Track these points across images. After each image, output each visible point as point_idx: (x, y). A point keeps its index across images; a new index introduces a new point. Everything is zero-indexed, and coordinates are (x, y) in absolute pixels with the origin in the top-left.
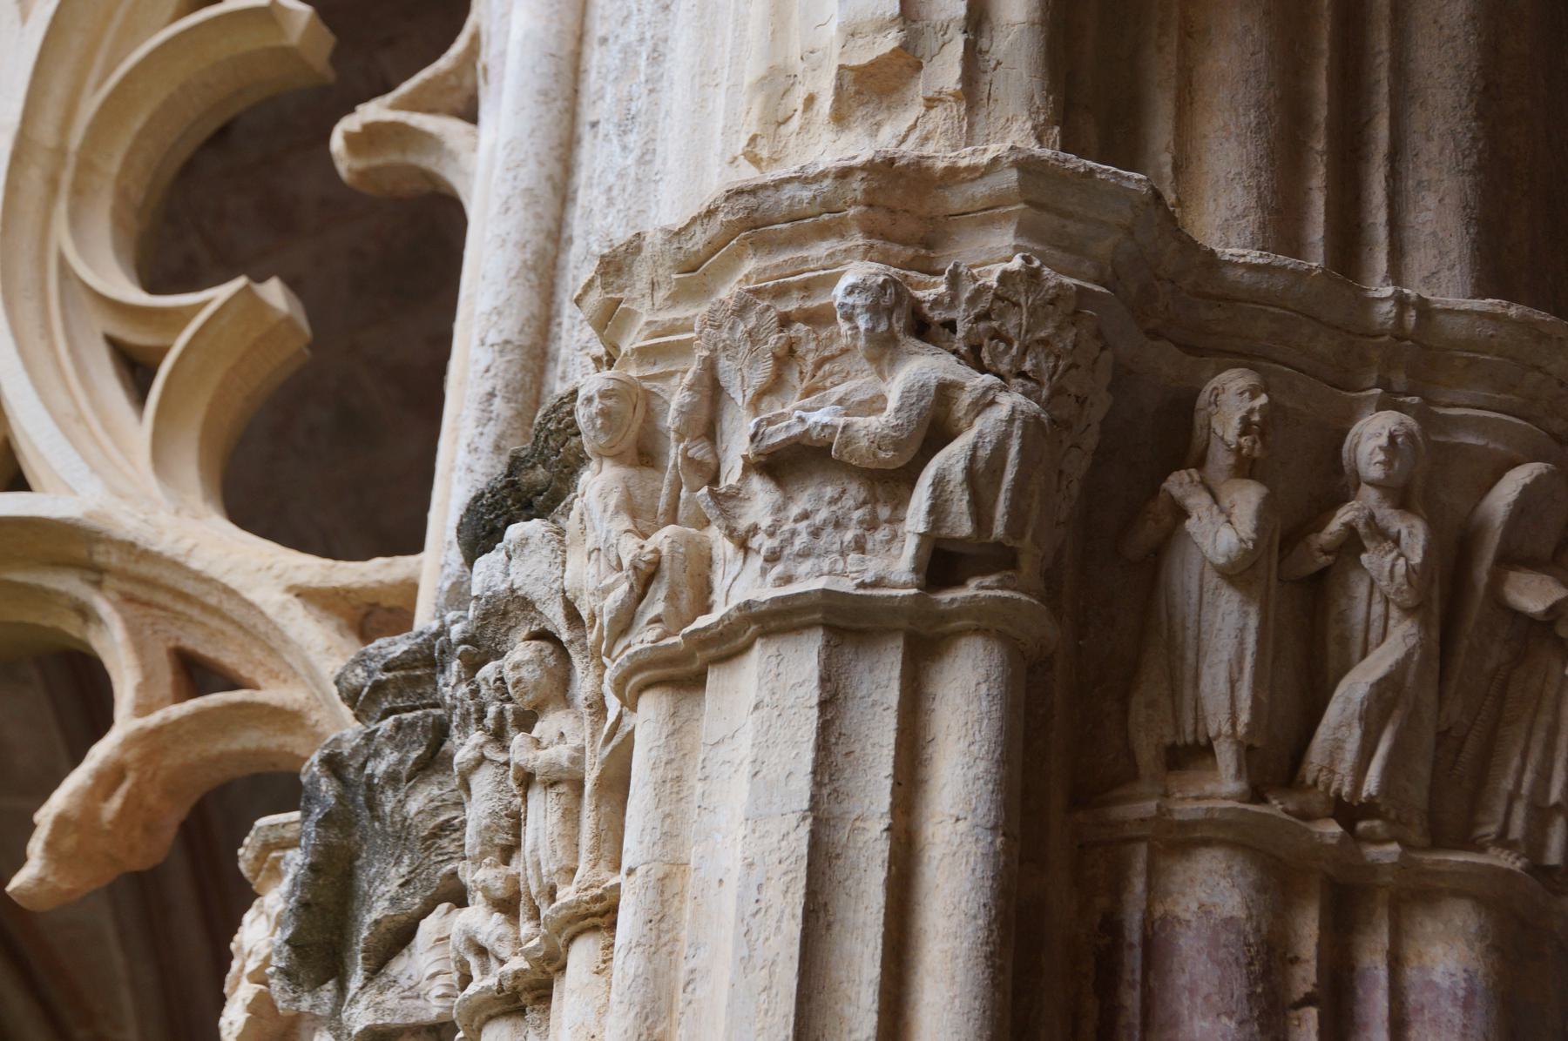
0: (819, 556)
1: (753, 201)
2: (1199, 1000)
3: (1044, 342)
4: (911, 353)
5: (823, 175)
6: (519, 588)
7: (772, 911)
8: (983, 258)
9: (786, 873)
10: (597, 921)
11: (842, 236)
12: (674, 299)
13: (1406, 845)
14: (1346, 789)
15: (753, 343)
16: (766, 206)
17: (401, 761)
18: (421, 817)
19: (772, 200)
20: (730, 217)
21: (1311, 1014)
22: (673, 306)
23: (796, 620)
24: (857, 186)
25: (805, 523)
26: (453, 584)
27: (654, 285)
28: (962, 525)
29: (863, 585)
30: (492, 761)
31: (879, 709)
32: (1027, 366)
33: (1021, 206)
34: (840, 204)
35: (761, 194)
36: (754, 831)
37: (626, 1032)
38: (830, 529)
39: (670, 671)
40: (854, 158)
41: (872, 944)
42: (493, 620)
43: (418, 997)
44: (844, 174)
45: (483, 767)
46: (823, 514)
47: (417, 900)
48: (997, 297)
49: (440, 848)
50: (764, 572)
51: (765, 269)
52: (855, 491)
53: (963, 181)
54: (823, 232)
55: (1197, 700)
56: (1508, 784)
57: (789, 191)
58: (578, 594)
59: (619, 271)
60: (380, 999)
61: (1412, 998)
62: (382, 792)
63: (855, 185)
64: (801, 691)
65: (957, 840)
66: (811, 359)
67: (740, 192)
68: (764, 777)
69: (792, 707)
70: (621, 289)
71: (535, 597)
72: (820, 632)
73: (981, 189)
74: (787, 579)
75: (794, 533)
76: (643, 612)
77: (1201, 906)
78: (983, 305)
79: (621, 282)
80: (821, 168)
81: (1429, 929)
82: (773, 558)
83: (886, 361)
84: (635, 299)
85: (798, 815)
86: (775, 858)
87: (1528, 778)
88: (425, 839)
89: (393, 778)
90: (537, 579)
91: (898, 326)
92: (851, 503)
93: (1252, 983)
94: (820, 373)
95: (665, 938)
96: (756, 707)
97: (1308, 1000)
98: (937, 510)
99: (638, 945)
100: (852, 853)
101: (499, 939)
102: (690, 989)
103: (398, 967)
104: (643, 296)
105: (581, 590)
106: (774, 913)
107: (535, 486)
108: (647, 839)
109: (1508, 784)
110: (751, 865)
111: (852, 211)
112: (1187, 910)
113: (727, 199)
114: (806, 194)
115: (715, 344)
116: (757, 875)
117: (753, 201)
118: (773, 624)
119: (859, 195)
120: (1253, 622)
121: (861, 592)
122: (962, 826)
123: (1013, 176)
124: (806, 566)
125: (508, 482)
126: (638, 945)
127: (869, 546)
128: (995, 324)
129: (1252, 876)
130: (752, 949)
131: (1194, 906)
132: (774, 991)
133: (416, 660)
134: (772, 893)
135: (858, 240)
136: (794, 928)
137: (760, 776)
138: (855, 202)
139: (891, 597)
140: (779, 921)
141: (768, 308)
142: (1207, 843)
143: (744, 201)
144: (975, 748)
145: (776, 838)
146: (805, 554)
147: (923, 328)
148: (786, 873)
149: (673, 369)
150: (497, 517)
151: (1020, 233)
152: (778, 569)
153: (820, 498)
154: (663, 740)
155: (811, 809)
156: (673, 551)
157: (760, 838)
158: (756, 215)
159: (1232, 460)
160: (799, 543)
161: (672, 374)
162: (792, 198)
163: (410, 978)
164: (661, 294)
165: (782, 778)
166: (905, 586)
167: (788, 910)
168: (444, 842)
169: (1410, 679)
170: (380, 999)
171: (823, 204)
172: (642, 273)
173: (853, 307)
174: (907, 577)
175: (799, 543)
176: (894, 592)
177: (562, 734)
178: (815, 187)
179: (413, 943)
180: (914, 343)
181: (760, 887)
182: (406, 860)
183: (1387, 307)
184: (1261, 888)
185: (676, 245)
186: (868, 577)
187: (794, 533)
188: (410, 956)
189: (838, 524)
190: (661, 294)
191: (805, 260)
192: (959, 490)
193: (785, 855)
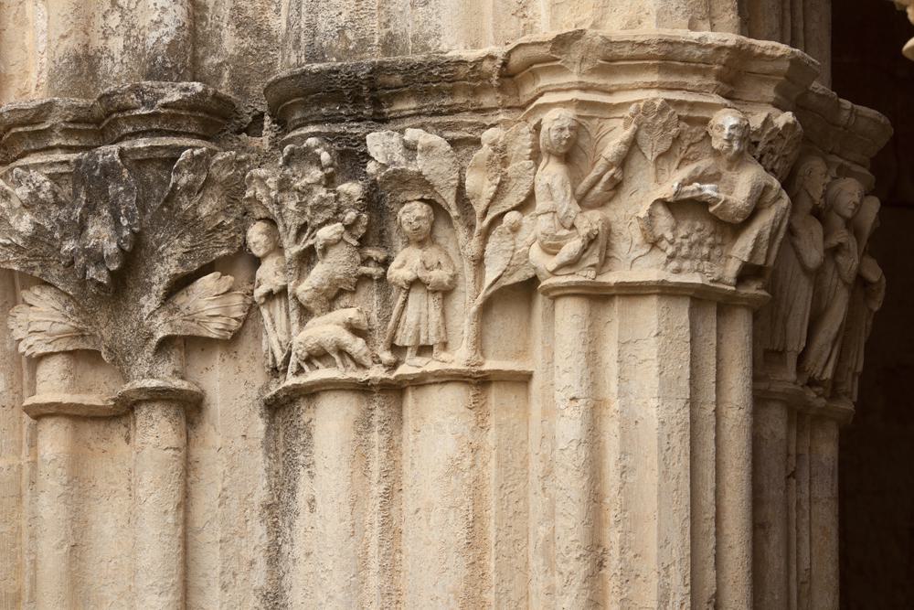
0: (692, 259)
1: (670, 48)
2: (771, 481)
3: (785, 156)
4: (747, 161)
5: (710, 46)
6: (427, 176)
7: (676, 449)
8: (759, 99)
9: (680, 431)
10: (472, 380)
11: (704, 76)
12: (593, 71)
14: (818, 374)
15: (665, 129)
16: (676, 52)
17: (195, 181)
18: (209, 218)
19: (680, 50)
20: (656, 53)
22: (590, 75)
23: (680, 292)
24: (724, 56)
25: (687, 241)
26: (172, 41)
27: (583, 60)
29: (712, 281)
30: (347, 243)
31: (707, 344)
32: (777, 167)
33: (783, 78)
34: (711, 62)
35: (675, 46)
36: (663, 404)
37: (584, 487)
38: (697, 245)
39: (594, 292)
40: (726, 41)
41: (711, 471)
42: (394, 182)
43: (193, 320)
44: (720, 49)
45: (340, 244)
46: (694, 237)
47: (196, 265)
48: (779, 134)
49: (216, 238)
50: (667, 263)
51: (664, 83)
52: (709, 227)
53: (763, 60)
54: (696, 71)
55: (785, 330)
57: (689, 48)
58: (476, 196)
59: (563, 44)
60: (170, 318)
62: (181, 195)
63: (723, 55)
64: (681, 332)
65: (740, 420)
66: (687, 143)
67: (665, 42)
68: (666, 376)
69: (677, 339)
70: (560, 54)
71: (436, 183)
72: (689, 300)
73: (769, 67)
74: (678, 271)
75: (682, 244)
76: (585, 259)
77: (772, 432)
78: (773, 137)
79: (562, 50)
80: (709, 42)
81: (821, 436)
82: (672, 257)
83: (735, 165)
84: (568, 62)
85: (685, 401)
86: (674, 421)
88: (209, 232)
89: (189, 189)
90: (438, 173)
92: (708, 233)
94: (689, 151)
95: (596, 440)
96: (657, 335)
99: (585, 442)
100: (700, 420)
101: (365, 355)
102: (624, 475)
103: (180, 300)
104: (575, 63)
105: (479, 196)
106: (677, 449)
107: (386, 84)
108: (584, 384)
110: (663, 422)
111: (716, 67)
112: (766, 434)
113: (659, 43)
114: (699, 53)
115: (642, 124)
116: (667, 429)
117: (670, 48)
118: (668, 292)
119: (723, 61)
120: (811, 295)
121: (712, 285)
122: (742, 412)
123: (787, 65)
124: (687, 264)
125: (370, 78)
126: (585, 442)
127: (712, 257)
128: (773, 146)
130: (667, 466)
131: (769, 433)
132: (680, 492)
133: (185, 106)
134: (675, 440)
135: (712, 81)
136: (686, 461)
137: (664, 374)
138: (719, 63)
139: (724, 290)
140: (679, 456)
141: (674, 112)
142: (774, 400)
143: (665, 47)
144: (746, 370)
145: (674, 411)
146: (685, 258)
148: (680, 431)
149: (596, 115)
150: (347, 88)
151: (777, 89)
152: (674, 264)
153: (693, 227)
154: (586, 330)
155: (690, 399)
156: (603, 229)
157: (667, 408)
158: (669, 55)
159: (810, 207)
160: (684, 251)
161: (593, 118)
162: (691, 52)
163: (188, 308)
164: (586, 66)
165: (675, 378)
166: (730, 285)
167: (683, 451)
168: (219, 235)
170: (170, 318)
171: (704, 59)
172: (576, 53)
173: (734, 135)
174: (732, 281)
175: (684, 251)
176: (726, 287)
177: (439, 263)
178: (703, 50)
179: (190, 287)
181: (669, 435)
182: (188, 238)
183: (846, 114)
185: (609, 48)
186: (715, 277)
187: (682, 244)
188: (188, 295)
189: (700, 243)
190: (586, 66)
191: (686, 84)
192: (765, 243)
193: (679, 421)
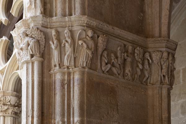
13: (72, 69)
21: (66, 84)
28: (31, 53)
56: (80, 60)
61: (75, 81)
87: (82, 59)
91: (25, 36)
93: (61, 83)
97: (66, 83)
98: (29, 52)
109: (80, 60)
129: (61, 74)
147: (27, 35)
169: (70, 54)
180: (26, 37)
184: (62, 75)
